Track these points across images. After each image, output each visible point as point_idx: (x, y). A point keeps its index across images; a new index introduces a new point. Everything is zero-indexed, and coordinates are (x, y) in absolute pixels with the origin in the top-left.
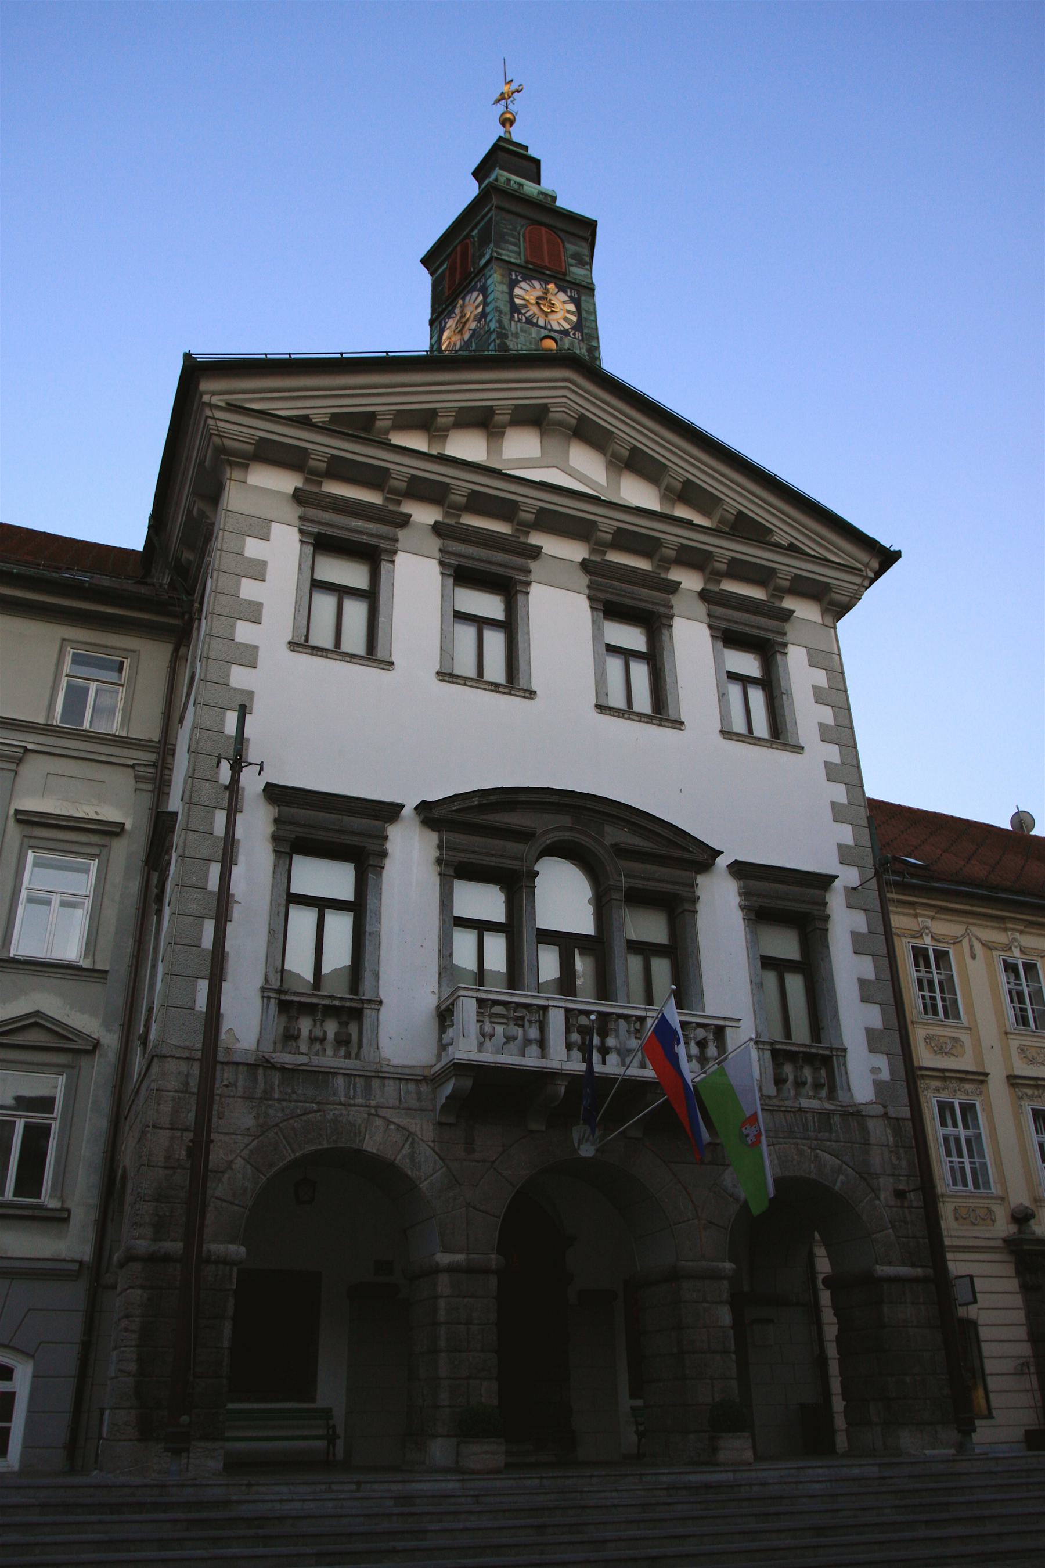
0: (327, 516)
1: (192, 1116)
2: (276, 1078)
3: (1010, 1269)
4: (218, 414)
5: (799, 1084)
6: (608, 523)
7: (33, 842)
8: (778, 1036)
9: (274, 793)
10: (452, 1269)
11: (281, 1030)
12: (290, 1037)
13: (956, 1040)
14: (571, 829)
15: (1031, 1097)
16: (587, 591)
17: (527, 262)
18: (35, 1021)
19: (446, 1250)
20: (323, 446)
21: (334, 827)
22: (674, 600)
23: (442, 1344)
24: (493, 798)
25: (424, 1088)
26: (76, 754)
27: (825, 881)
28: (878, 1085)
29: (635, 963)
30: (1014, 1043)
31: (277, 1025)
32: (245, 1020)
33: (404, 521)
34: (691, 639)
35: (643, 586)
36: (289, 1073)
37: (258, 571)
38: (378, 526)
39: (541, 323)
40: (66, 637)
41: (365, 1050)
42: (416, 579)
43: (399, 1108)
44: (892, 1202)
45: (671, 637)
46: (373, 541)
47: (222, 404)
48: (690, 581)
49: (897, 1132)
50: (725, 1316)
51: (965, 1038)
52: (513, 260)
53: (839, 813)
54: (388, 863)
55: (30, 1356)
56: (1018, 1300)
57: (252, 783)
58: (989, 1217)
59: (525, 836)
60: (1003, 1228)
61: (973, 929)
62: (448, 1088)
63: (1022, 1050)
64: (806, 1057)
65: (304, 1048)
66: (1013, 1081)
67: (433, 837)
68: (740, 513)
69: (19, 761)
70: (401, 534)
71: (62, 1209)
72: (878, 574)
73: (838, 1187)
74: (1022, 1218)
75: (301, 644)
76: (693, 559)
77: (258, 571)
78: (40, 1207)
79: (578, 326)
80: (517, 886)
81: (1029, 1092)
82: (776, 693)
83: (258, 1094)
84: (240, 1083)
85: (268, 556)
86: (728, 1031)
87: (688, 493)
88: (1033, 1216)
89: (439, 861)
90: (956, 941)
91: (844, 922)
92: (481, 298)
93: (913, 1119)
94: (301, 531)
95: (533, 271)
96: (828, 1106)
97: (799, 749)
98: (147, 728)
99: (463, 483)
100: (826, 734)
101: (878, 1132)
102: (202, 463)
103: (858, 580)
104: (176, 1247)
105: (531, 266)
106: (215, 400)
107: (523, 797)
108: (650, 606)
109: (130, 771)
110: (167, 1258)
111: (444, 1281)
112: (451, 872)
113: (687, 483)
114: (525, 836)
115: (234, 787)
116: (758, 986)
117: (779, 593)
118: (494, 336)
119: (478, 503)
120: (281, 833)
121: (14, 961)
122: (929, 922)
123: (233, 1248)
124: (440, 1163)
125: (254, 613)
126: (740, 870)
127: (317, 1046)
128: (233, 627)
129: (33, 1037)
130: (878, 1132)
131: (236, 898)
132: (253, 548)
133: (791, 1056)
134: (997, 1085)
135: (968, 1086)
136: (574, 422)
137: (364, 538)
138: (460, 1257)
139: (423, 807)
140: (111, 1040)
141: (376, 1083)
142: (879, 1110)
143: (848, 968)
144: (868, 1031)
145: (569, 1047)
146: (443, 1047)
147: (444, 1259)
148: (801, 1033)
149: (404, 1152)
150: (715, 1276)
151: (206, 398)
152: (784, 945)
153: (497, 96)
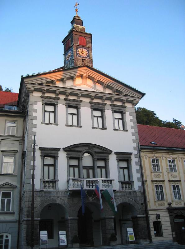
0: (46, 99)
1: (31, 200)
2: (43, 193)
3: (167, 213)
4: (28, 85)
5: (126, 187)
6: (93, 95)
8: (123, 180)
9: (41, 149)
10: (71, 220)
11: (44, 186)
12: (45, 187)
13: (159, 175)
14: (88, 149)
15: (172, 184)
16: (90, 107)
18: (7, 184)
19: (69, 217)
21: (50, 153)
22: (105, 106)
23: (70, 230)
25: (66, 193)
27: (131, 154)
28: (139, 187)
29: (99, 170)
30: (170, 174)
31: (43, 185)
32: (38, 185)
33: (59, 99)
34: (108, 113)
36: (45, 192)
37: (36, 111)
39: (82, 57)
40: (6, 119)
41: (56, 188)
42: (61, 108)
44: (141, 205)
46: (54, 103)
48: (108, 103)
49: (142, 194)
50: (113, 224)
51: (161, 174)
52: (77, 44)
53: (134, 141)
54: (59, 158)
55: (11, 234)
56: (169, 218)
57: (37, 148)
58: (164, 204)
59: (80, 151)
60: (166, 206)
61: (163, 155)
63: (171, 175)
64: (127, 183)
65: (47, 188)
66: (169, 181)
67: (66, 153)
70: (59, 101)
72: (142, 98)
73: (131, 204)
74: (170, 204)
75: (43, 123)
76: (108, 99)
77: (36, 111)
78: (10, 212)
79: (89, 56)
80: (79, 159)
81: (172, 183)
83: (41, 196)
84: (38, 194)
85: (37, 107)
86: (113, 181)
87: (108, 87)
88: (171, 204)
89: (67, 157)
90: (160, 157)
92: (71, 52)
93: (143, 192)
94: (42, 103)
95: (80, 46)
96: (130, 191)
97: (127, 131)
98: (20, 134)
99: (68, 91)
101: (139, 194)
102: (25, 92)
103: (138, 99)
104: (30, 219)
106: (27, 83)
107: (80, 145)
108: (101, 108)
110: (29, 220)
111: (69, 221)
112: (69, 158)
114: (80, 151)
115: (34, 148)
116: (119, 172)
117: (124, 103)
119: (71, 94)
120: (42, 155)
121: (3, 174)
122: (155, 155)
123: (38, 218)
125: (35, 118)
126: (116, 153)
127: (49, 188)
128: (32, 121)
129: (6, 186)
130: (139, 194)
132: (35, 107)
133: (125, 183)
134: (166, 182)
135: (161, 183)
137: (53, 103)
138: (72, 218)
139: (64, 148)
140: (19, 186)
141: (58, 193)
142: (139, 191)
143: (135, 167)
144: (138, 178)
145: (87, 186)
146: (68, 187)
147: (69, 218)
148: (127, 179)
150: (111, 218)
151: (25, 82)
152: (124, 165)
153: (75, 5)
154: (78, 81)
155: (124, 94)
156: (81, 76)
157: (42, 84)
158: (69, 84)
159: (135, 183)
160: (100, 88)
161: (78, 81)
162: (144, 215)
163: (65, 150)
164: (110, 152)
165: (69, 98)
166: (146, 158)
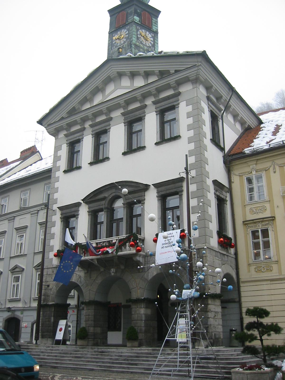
6: (122, 102)
14: (115, 192)
24: (95, 193)
35: (137, 111)
38: (80, 133)
43: (78, 271)
45: (144, 122)
47: (47, 126)
54: (79, 216)
59: (104, 199)
68: (160, 71)
87: (147, 75)
99: (89, 113)
100: (190, 127)
103: (196, 69)
105: (117, 28)
108: (139, 116)
124: (85, 281)
128: (55, 174)
131: (55, 233)
136: (117, 75)
149: (79, 280)
155: (172, 71)
157: (62, 118)
158: (98, 99)
160: (139, 82)
161: (110, 88)
164: (146, 187)
166: (274, 168)
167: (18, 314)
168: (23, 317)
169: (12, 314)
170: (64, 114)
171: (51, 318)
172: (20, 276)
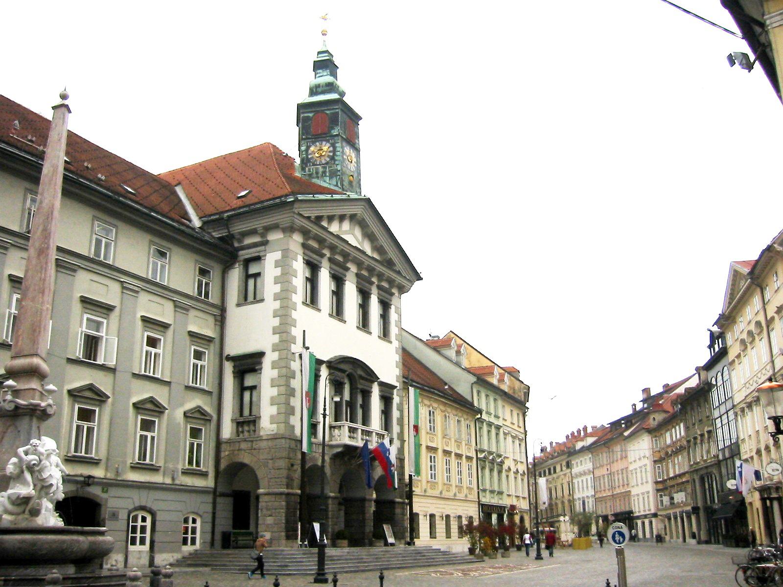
4: (295, 216)
7: (193, 343)
17: (347, 138)
18: (199, 410)
20: (315, 230)
23: (330, 516)
26: (203, 309)
55: (201, 516)
59: (343, 371)
62: (340, 450)
69: (187, 310)
71: (207, 472)
82: (387, 321)
87: (379, 249)
91: (396, 399)
97: (391, 342)
99: (341, 246)
109: (213, 317)
113: (382, 246)
118: (339, 173)
137: (315, 262)
140: (215, 417)
147: (332, 495)
154: (346, 225)
156: (353, 217)
159: (394, 440)
160: (367, 248)
161: (346, 225)
162: (401, 498)
163: (331, 365)
165: (335, 257)
167: (95, 491)
168: (106, 500)
169: (77, 490)
170: (313, 214)
171: (296, 512)
172: (97, 410)
